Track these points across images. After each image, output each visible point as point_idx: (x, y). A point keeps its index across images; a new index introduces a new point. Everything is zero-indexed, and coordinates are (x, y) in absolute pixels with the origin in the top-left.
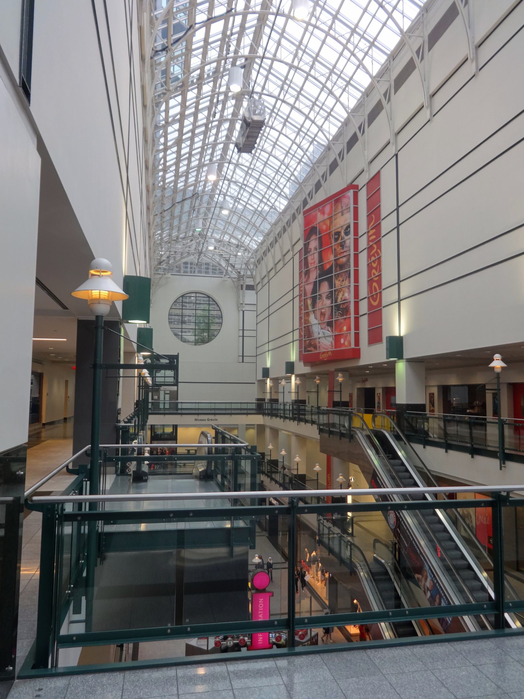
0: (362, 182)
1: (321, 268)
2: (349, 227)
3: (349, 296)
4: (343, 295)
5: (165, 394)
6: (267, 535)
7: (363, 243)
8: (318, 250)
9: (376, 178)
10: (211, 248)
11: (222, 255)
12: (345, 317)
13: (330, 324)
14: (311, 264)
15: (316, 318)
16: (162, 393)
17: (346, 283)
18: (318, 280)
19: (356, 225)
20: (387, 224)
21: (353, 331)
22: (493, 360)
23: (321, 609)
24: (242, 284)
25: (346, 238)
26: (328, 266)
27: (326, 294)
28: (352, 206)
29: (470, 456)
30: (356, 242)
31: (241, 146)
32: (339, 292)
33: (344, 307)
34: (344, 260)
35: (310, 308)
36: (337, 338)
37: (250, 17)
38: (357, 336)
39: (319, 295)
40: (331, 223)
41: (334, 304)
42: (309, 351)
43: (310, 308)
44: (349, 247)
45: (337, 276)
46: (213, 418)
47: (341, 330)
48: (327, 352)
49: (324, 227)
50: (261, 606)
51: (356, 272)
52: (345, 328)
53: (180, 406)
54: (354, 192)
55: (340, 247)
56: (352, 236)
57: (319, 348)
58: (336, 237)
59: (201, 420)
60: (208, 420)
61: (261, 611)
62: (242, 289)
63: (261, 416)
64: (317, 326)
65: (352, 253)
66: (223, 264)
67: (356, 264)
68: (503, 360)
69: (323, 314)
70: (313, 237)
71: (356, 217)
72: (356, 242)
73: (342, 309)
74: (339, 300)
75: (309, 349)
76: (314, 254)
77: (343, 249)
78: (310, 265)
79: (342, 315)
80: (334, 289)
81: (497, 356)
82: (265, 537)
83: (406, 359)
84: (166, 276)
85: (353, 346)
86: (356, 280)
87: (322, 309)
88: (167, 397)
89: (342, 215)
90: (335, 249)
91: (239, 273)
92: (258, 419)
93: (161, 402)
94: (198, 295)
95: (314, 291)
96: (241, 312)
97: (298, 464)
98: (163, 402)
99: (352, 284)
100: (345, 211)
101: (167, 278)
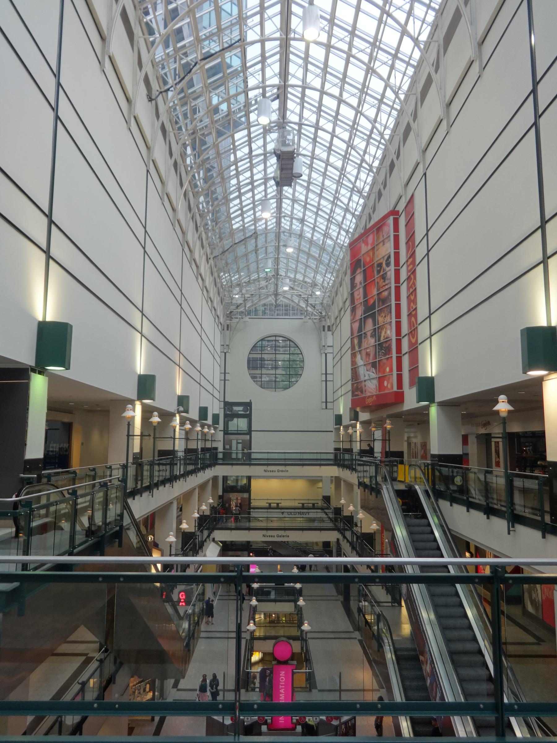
0: (401, 207)
1: (366, 302)
2: (389, 257)
3: (391, 333)
4: (386, 332)
5: (238, 443)
6: (343, 600)
7: (404, 275)
8: (363, 285)
9: (411, 200)
10: (286, 288)
11: (300, 295)
12: (388, 357)
13: (374, 365)
14: (357, 300)
15: (362, 359)
17: (388, 319)
18: (363, 316)
19: (397, 255)
20: (420, 252)
21: (395, 372)
22: (497, 402)
23: (378, 688)
24: (324, 324)
25: (387, 269)
26: (372, 302)
27: (371, 332)
28: (392, 234)
29: (486, 516)
30: (397, 273)
31: (279, 180)
32: (382, 329)
33: (387, 345)
34: (386, 293)
35: (357, 348)
36: (381, 380)
37: (269, 45)
38: (400, 378)
39: (364, 333)
40: (373, 254)
41: (377, 343)
42: (358, 395)
43: (357, 348)
44: (390, 279)
45: (380, 311)
46: (284, 470)
47: (384, 371)
48: (372, 396)
49: (368, 259)
51: (398, 306)
52: (388, 369)
53: (254, 456)
54: (394, 218)
55: (382, 280)
56: (392, 267)
57: (365, 391)
58: (379, 269)
59: (271, 471)
60: (278, 471)
61: (282, 685)
62: (324, 330)
63: (336, 467)
64: (363, 367)
65: (393, 285)
66: (303, 305)
67: (398, 298)
68: (510, 402)
69: (368, 354)
70: (359, 271)
71: (397, 245)
72: (397, 273)
73: (385, 348)
74: (382, 338)
75: (357, 393)
76: (359, 289)
77: (384, 281)
78: (356, 301)
79: (385, 355)
80: (377, 326)
81: (502, 398)
82: (340, 602)
83: (438, 403)
84: (244, 320)
85: (395, 389)
86: (398, 315)
87: (367, 348)
88: (240, 446)
89: (384, 244)
90: (378, 283)
91: (321, 313)
92: (334, 471)
94: (277, 338)
95: (360, 330)
96: (324, 355)
97: (361, 521)
98: (235, 452)
99: (394, 320)
100: (386, 240)
101: (245, 322)
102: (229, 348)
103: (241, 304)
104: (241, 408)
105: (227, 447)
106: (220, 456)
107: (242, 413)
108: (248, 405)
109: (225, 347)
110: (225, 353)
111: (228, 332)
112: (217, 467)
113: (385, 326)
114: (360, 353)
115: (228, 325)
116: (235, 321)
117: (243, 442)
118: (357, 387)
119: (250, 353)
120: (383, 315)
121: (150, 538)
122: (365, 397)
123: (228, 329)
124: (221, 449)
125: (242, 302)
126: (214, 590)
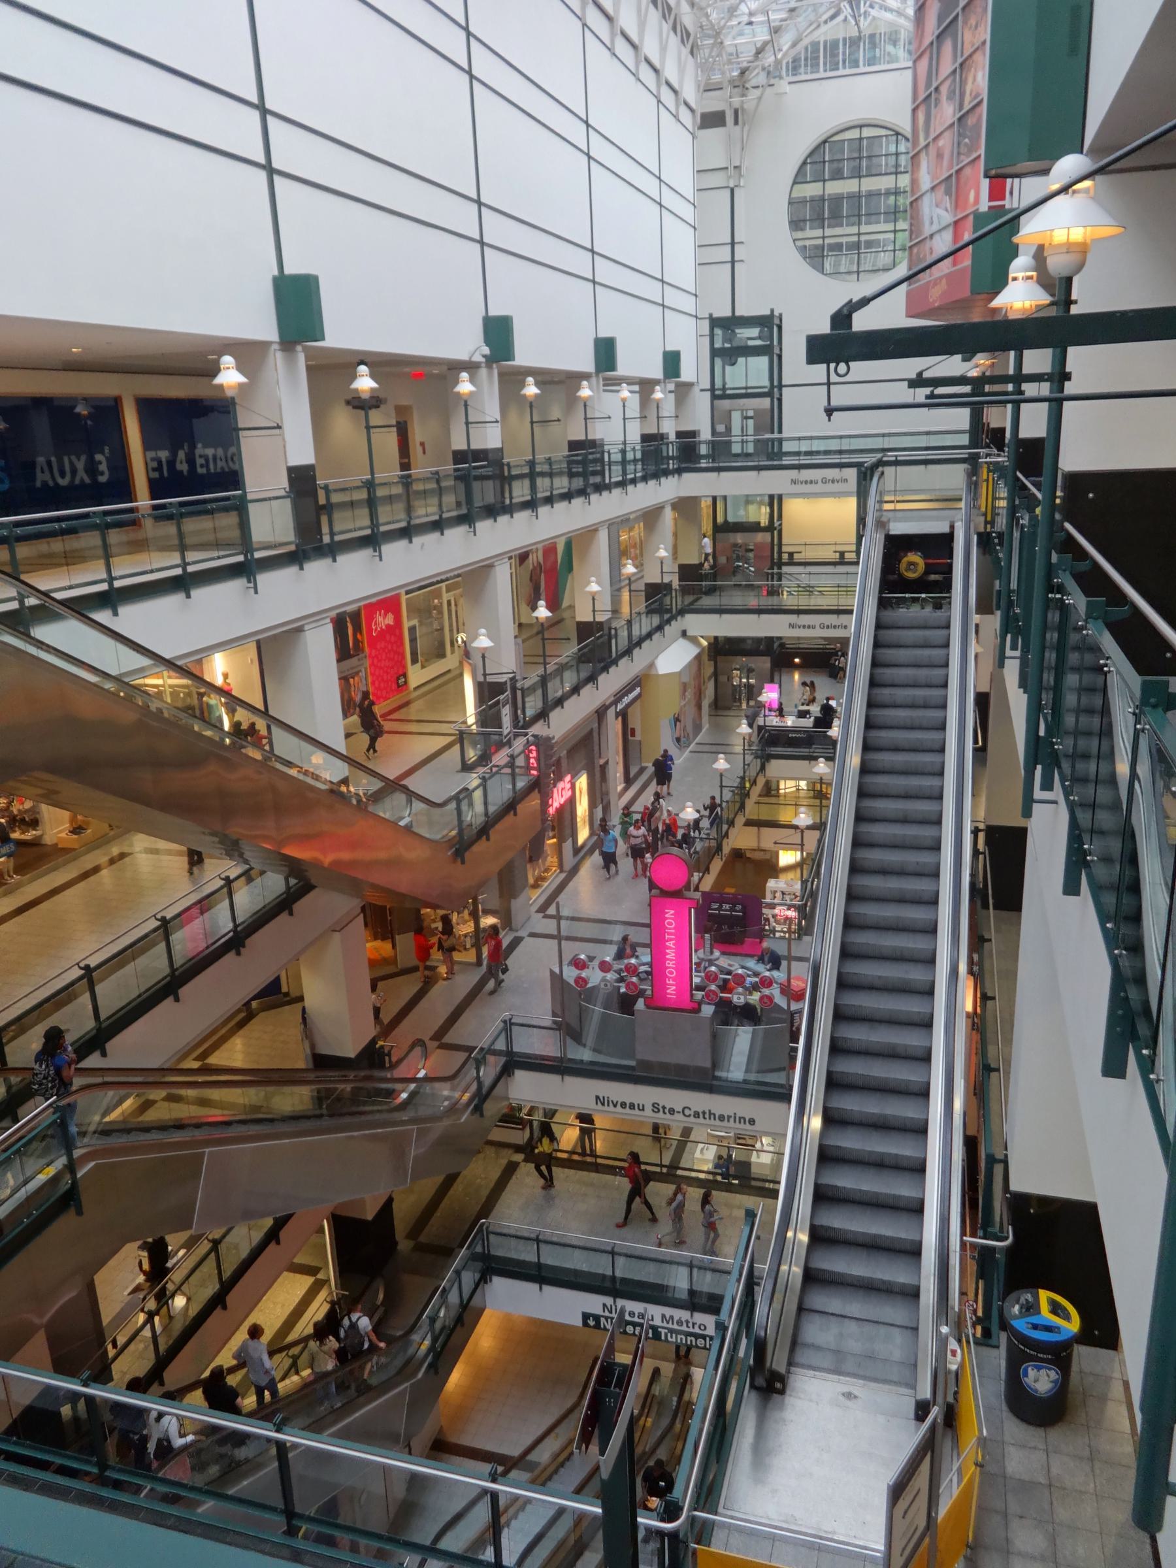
16: (736, 417)
18: (937, 33)
39: (937, 89)
46: (837, 477)
48: (941, 278)
50: (670, 924)
53: (787, 447)
59: (806, 482)
60: (825, 481)
61: (669, 934)
69: (940, 156)
74: (967, 98)
80: (960, 60)
93: (733, 439)
98: (739, 439)
102: (740, 176)
103: (765, 44)
104: (754, 332)
105: (721, 428)
106: (703, 450)
107: (759, 343)
108: (769, 323)
109: (731, 171)
110: (732, 191)
111: (738, 128)
112: (687, 476)
113: (975, 57)
114: (927, 154)
115: (736, 112)
116: (753, 94)
117: (758, 413)
118: (918, 253)
119: (795, 183)
120: (973, 22)
121: (461, 638)
122: (928, 283)
123: (736, 123)
124: (706, 435)
125: (768, 38)
126: (677, 735)
